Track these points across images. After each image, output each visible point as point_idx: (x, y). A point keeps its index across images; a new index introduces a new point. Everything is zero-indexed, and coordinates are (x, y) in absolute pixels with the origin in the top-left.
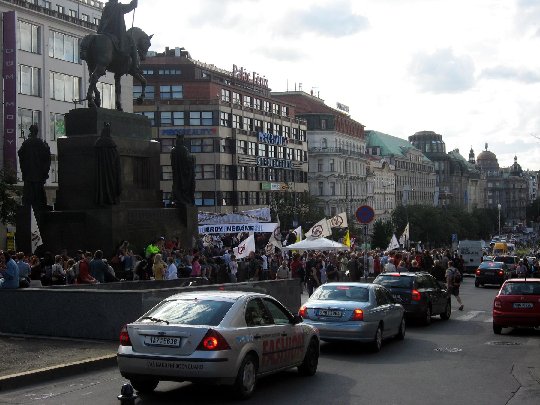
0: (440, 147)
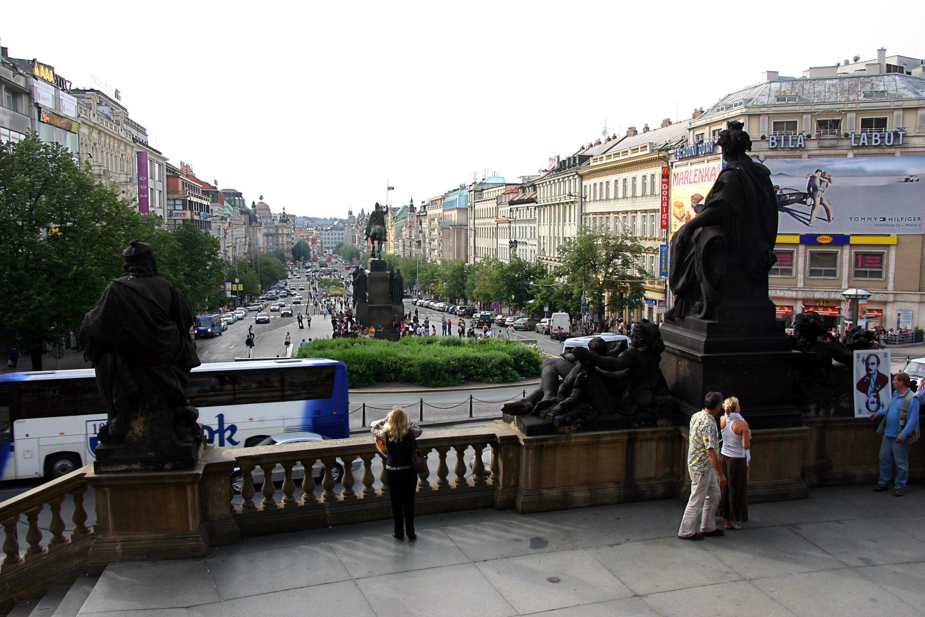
0: (242, 203)
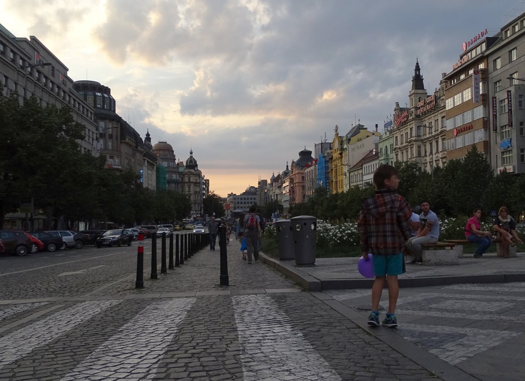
0: (107, 102)
